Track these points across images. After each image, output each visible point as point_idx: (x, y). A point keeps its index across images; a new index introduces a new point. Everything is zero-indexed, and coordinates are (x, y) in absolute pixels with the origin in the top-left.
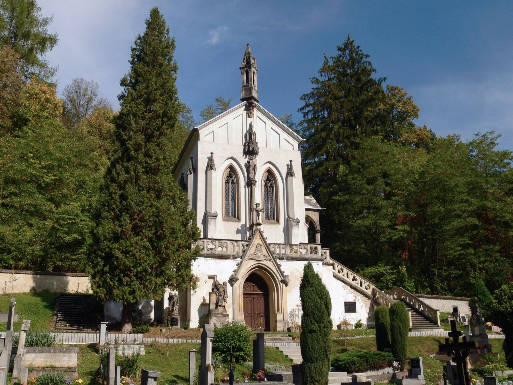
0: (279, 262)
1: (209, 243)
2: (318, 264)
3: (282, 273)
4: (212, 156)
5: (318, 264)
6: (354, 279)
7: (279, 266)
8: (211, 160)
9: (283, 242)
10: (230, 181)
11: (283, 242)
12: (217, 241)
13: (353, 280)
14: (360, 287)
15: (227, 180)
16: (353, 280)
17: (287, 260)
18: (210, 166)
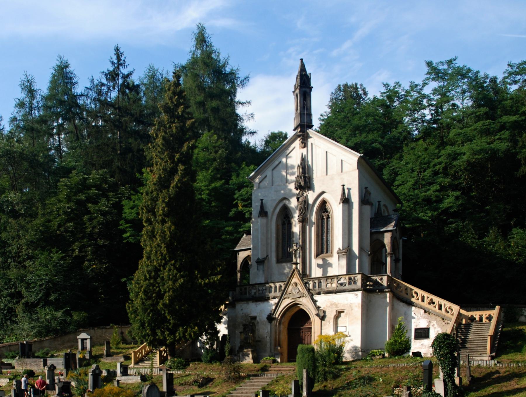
0: (316, 297)
1: (250, 288)
2: (357, 295)
3: (318, 308)
4: (262, 203)
5: (357, 295)
6: (432, 302)
7: (315, 302)
8: (262, 206)
9: (345, 273)
10: (286, 223)
11: (345, 273)
12: (257, 286)
13: (429, 303)
14: (440, 311)
15: (284, 222)
16: (429, 303)
17: (325, 294)
18: (263, 213)
